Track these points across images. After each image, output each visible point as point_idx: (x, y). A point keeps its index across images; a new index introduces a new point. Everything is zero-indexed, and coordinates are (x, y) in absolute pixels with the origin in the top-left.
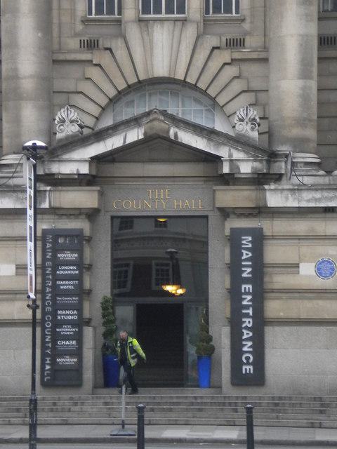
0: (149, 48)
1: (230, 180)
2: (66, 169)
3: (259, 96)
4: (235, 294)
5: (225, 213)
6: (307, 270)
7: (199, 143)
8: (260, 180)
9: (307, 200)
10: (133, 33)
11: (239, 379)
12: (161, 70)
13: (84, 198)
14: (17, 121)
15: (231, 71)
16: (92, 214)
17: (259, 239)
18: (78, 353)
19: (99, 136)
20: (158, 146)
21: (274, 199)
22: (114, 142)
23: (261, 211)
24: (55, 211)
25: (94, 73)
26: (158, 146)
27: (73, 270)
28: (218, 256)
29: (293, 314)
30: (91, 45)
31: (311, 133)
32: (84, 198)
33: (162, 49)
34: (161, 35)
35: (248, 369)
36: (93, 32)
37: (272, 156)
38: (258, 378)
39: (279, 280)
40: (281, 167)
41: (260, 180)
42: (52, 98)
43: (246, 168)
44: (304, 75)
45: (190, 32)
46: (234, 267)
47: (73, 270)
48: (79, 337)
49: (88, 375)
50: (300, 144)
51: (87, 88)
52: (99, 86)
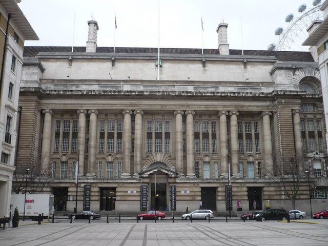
0: (157, 157)
1: (171, 178)
2: (145, 176)
3: (175, 164)
4: (171, 196)
5: (169, 183)
6: (183, 192)
7: (166, 172)
8: (175, 178)
9: (182, 181)
10: (154, 155)
11: (172, 209)
12: (158, 161)
13: (147, 180)
14: (137, 168)
15: (169, 161)
16: (148, 183)
17: (175, 187)
18: (146, 205)
19: (150, 171)
20: (159, 172)
21: (177, 181)
22: (152, 172)
23: (175, 183)
24: (143, 182)
25: (148, 161)
26: (159, 172)
27: (145, 192)
28: (168, 190)
29: (181, 199)
30: (147, 156)
31: (182, 170)
32: (147, 180)
33: (159, 157)
34: (159, 155)
35: (173, 208)
36: (148, 155)
37: (177, 174)
38: (175, 209)
39: (178, 194)
40: (179, 176)
41: (175, 178)
42: (142, 165)
43: (173, 176)
44: (181, 161)
45: (163, 155)
46: (171, 192)
47: (145, 192)
48: (146, 203)
49: (148, 209)
50: (181, 172)
51: (147, 163)
52: (149, 163)
